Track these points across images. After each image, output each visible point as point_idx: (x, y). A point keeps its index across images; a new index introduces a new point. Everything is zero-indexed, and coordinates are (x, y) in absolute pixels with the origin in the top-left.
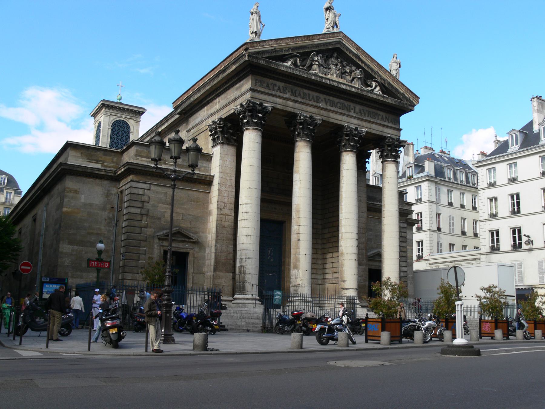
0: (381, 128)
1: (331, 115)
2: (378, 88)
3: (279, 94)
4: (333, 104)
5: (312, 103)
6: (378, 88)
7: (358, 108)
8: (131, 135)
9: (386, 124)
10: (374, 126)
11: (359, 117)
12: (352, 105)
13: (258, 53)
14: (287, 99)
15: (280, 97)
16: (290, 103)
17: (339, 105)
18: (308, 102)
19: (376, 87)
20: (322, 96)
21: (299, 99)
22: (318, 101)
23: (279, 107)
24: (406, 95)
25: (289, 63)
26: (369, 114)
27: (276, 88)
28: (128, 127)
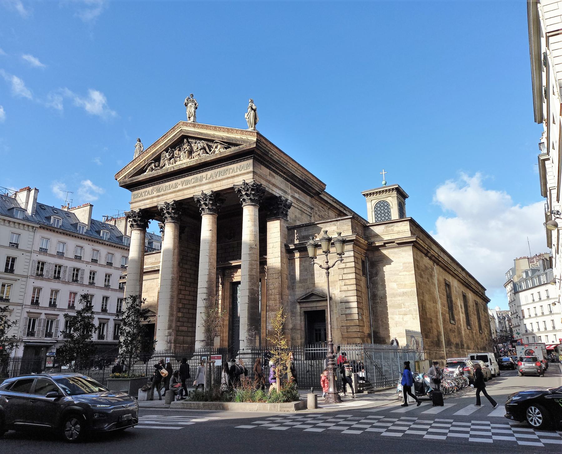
0: (231, 180)
1: (185, 192)
2: (219, 146)
3: (149, 196)
4: (188, 182)
5: (172, 190)
6: (219, 146)
7: (209, 173)
8: (392, 210)
9: (239, 172)
10: (224, 182)
11: (210, 180)
12: (204, 174)
13: (125, 177)
14: (152, 198)
15: (147, 199)
16: (155, 199)
17: (193, 180)
18: (169, 191)
19: (216, 147)
20: (179, 181)
21: (162, 193)
22: (176, 186)
23: (148, 206)
24: (244, 138)
25: (147, 171)
26: (220, 173)
27: (146, 194)
28: (388, 205)
